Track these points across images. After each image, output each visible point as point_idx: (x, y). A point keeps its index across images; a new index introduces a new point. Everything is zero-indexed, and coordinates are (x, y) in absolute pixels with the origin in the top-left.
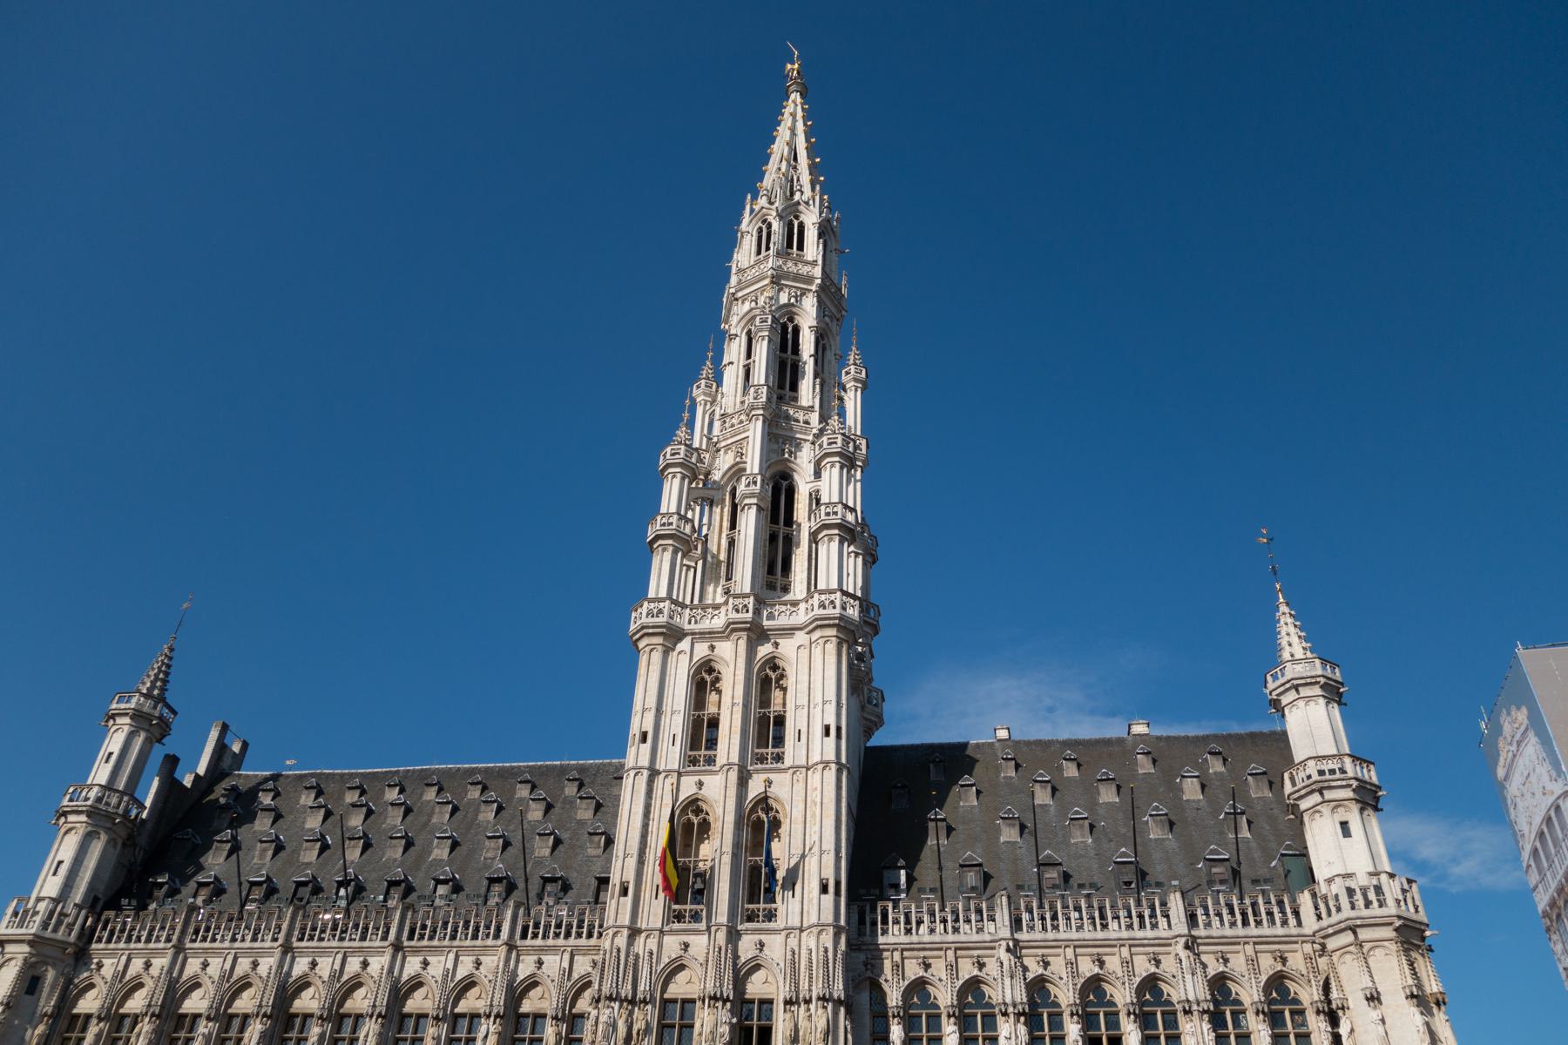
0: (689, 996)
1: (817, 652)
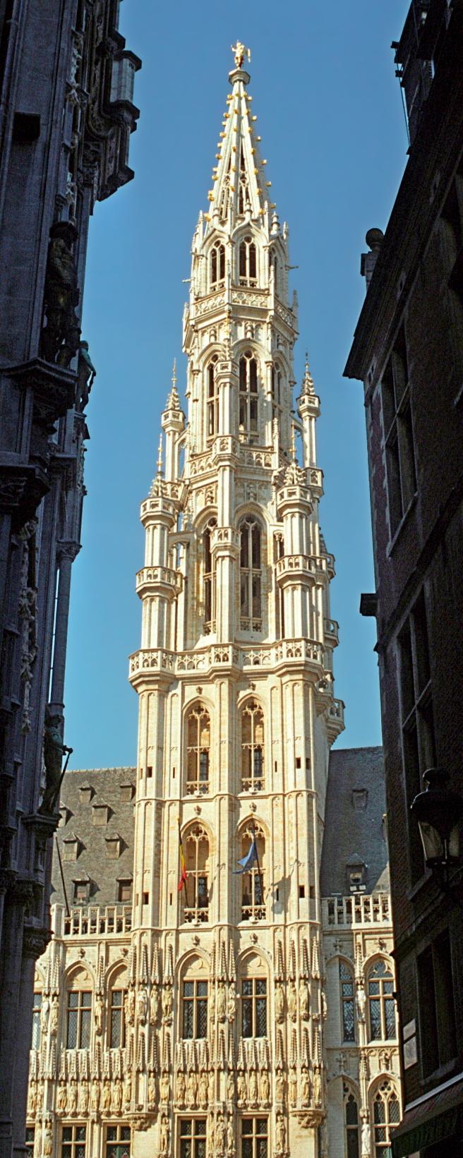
0: (202, 978)
1: (288, 692)
